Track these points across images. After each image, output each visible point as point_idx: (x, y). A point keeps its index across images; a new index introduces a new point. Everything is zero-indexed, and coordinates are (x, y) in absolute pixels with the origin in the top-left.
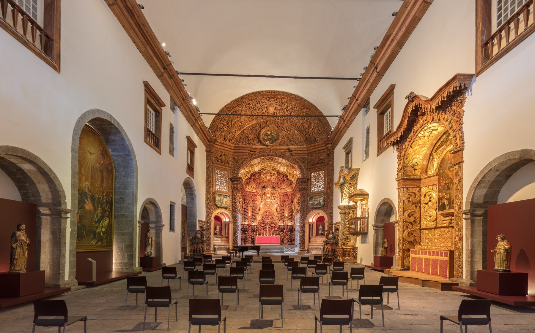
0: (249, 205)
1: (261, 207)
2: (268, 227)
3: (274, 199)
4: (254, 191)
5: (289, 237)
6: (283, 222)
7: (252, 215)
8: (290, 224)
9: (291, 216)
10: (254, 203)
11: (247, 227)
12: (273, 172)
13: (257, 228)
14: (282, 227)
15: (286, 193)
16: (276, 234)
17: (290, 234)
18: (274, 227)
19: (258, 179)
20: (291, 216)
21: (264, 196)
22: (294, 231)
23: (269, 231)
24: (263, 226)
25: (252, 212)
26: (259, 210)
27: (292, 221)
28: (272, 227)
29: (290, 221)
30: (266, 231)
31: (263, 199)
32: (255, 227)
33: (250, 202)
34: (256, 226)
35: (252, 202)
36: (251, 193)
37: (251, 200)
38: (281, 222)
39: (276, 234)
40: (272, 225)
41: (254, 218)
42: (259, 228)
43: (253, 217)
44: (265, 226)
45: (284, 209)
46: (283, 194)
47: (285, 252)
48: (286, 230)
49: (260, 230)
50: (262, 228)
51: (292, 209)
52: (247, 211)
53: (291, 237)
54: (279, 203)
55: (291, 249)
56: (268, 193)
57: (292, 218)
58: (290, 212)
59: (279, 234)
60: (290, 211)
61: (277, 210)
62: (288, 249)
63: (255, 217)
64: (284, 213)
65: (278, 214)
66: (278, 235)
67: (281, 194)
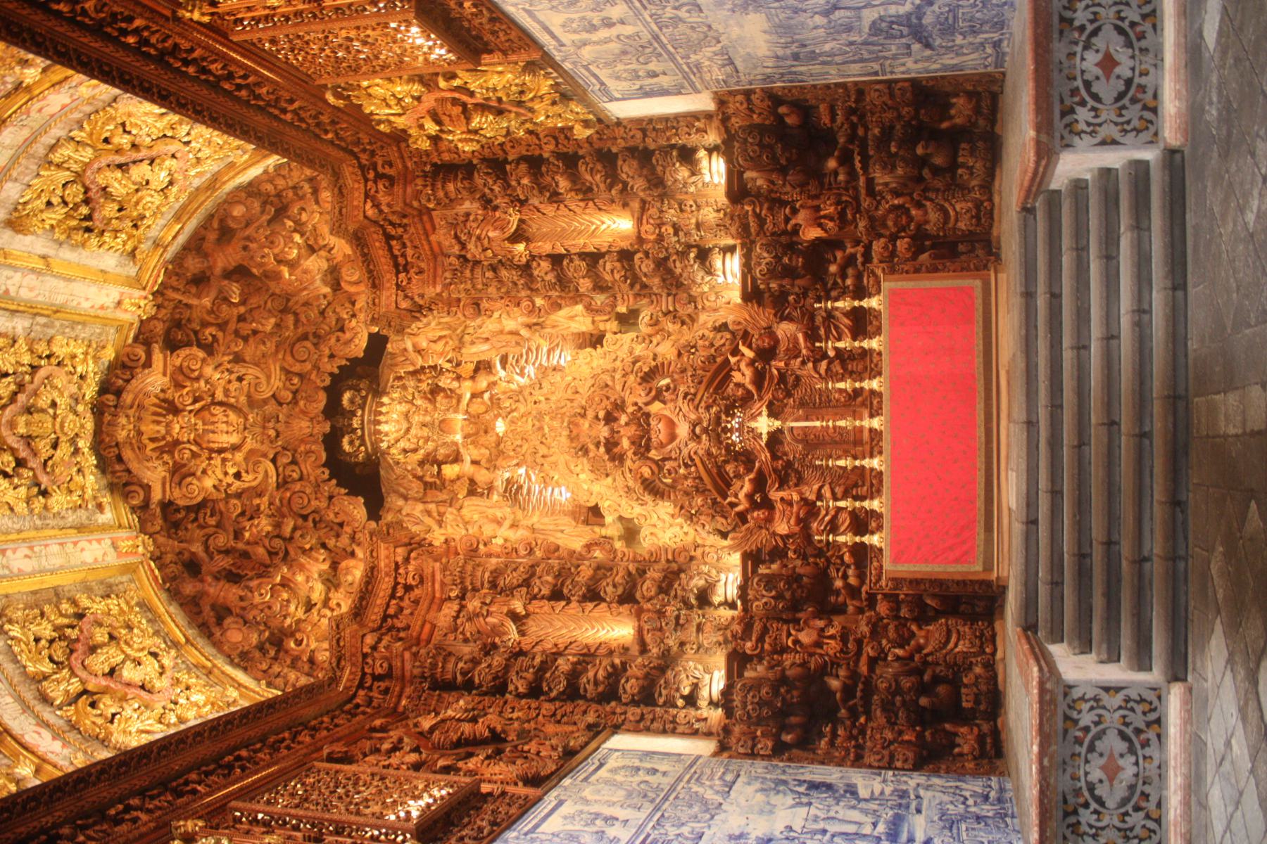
0: (497, 631)
1: (563, 495)
2: (764, 424)
3: (483, 367)
4: (355, 572)
5: (889, 166)
6: (704, 255)
7: (627, 598)
8: (715, 171)
9: (627, 169)
10: (497, 573)
11: (756, 685)
12: (154, 380)
13: (777, 553)
14: (764, 257)
15: (358, 240)
16: (862, 323)
17: (846, 159)
18: (766, 355)
19: (238, 535)
20: (627, 169)
21: (450, 471)
22: (803, 107)
23: (816, 405)
24: (760, 484)
25: (593, 595)
26: (594, 514)
27: (687, 155)
28: (759, 379)
29: (683, 173)
30: (812, 442)
31: (482, 476)
32: (769, 581)
33: (469, 628)
34: (752, 559)
35: (473, 604)
36: (374, 615)
37: (450, 609)
38: (702, 284)
39: (862, 323)
40: (743, 376)
41: (665, 587)
42: (782, 528)
43: (647, 587)
44: (746, 458)
45: (556, 260)
46: (389, 279)
47: (1171, 133)
48: (801, 218)
49: (804, 523)
50: (775, 495)
51: (535, 164)
52: (563, 665)
53: (887, 133)
54: (510, 325)
55: (1109, 41)
56: (444, 427)
57: (644, 156)
58: (574, 178)
59: (860, 293)
60: (563, 184)
61: (596, 340)
62: (1107, 89)
63: (654, 574)
64: (593, 258)
65: (627, 320)
66: (873, 303)
67: (388, 296)
